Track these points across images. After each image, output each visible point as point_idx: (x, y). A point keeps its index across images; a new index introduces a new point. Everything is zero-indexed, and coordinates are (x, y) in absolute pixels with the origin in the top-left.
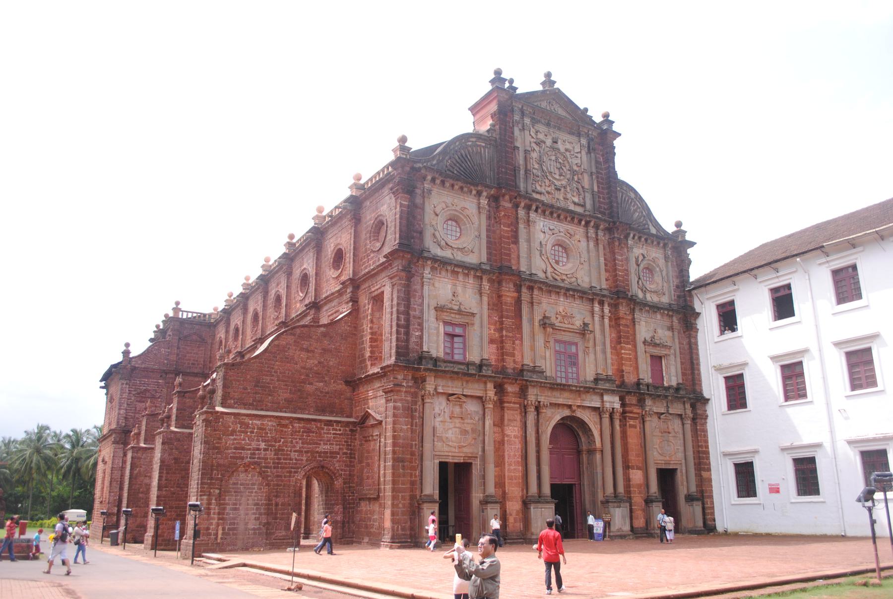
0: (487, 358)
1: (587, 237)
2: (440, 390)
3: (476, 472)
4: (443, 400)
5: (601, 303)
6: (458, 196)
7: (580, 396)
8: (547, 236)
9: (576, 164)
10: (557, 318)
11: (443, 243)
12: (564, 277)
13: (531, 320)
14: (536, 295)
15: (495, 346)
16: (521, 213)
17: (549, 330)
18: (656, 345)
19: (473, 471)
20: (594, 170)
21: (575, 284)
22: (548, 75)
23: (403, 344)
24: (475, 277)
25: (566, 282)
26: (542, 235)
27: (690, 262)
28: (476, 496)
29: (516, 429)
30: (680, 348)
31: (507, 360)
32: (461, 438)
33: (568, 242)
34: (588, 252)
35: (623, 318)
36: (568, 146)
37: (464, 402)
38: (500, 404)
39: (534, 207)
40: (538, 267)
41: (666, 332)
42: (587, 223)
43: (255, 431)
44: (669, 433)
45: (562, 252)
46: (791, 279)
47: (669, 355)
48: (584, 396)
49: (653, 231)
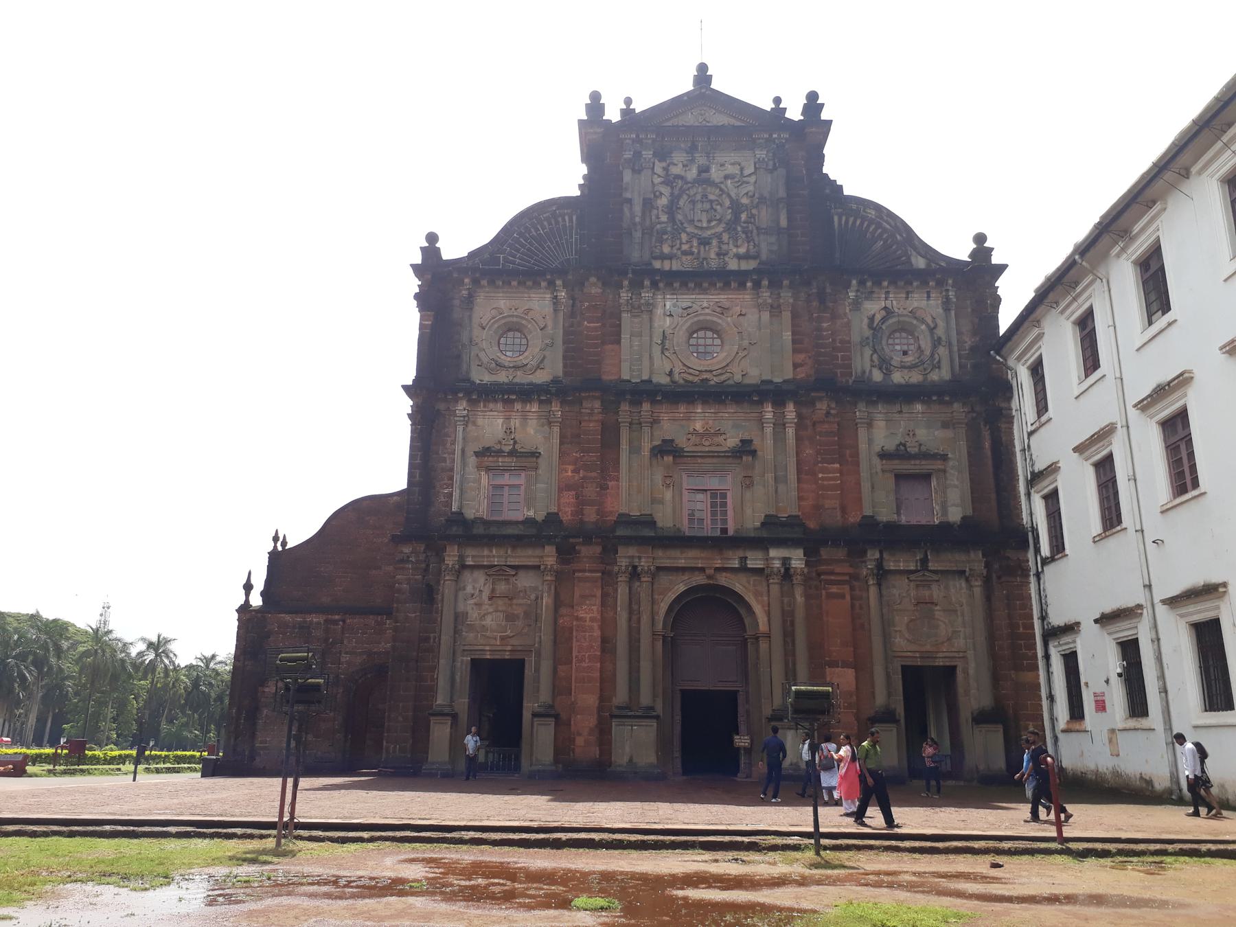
0: (556, 511)
1: (760, 307)
2: (469, 562)
3: (529, 672)
4: (480, 576)
6: (519, 295)
9: (747, 194)
10: (689, 439)
12: (705, 376)
13: (635, 450)
14: (646, 411)
15: (574, 493)
17: (669, 459)
19: (526, 671)
20: (782, 193)
21: (731, 382)
22: (703, 68)
23: (418, 507)
24: (541, 402)
25: (712, 383)
27: (997, 300)
28: (529, 707)
29: (595, 608)
31: (585, 512)
32: (506, 626)
33: (720, 321)
35: (823, 422)
36: (730, 169)
37: (514, 576)
39: (647, 283)
40: (659, 370)
41: (936, 433)
42: (757, 285)
43: (296, 631)
44: (932, 603)
45: (713, 338)
46: (1090, 297)
47: (944, 471)
48: (730, 553)
49: (920, 263)
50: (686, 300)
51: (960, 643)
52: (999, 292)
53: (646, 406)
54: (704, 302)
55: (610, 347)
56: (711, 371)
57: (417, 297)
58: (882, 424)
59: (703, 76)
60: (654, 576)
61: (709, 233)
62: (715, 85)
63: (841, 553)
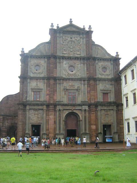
1: (81, 63)
3: (41, 127)
4: (32, 110)
5: (84, 80)
7: (74, 106)
8: (67, 65)
11: (33, 72)
12: (72, 75)
16: (58, 60)
18: (105, 90)
20: (85, 43)
22: (71, 19)
24: (43, 79)
26: (65, 65)
27: (119, 64)
30: (115, 90)
34: (81, 67)
36: (76, 38)
38: (48, 110)
48: (76, 107)
49: (107, 57)
50: (68, 61)
51: (112, 121)
52: (120, 62)
53: (61, 81)
54: (71, 62)
55: (55, 70)
56: (73, 74)
57: (21, 60)
58: (101, 84)
59: (71, 21)
60: (63, 111)
61: (72, 49)
62: (73, 23)
63: (94, 107)
